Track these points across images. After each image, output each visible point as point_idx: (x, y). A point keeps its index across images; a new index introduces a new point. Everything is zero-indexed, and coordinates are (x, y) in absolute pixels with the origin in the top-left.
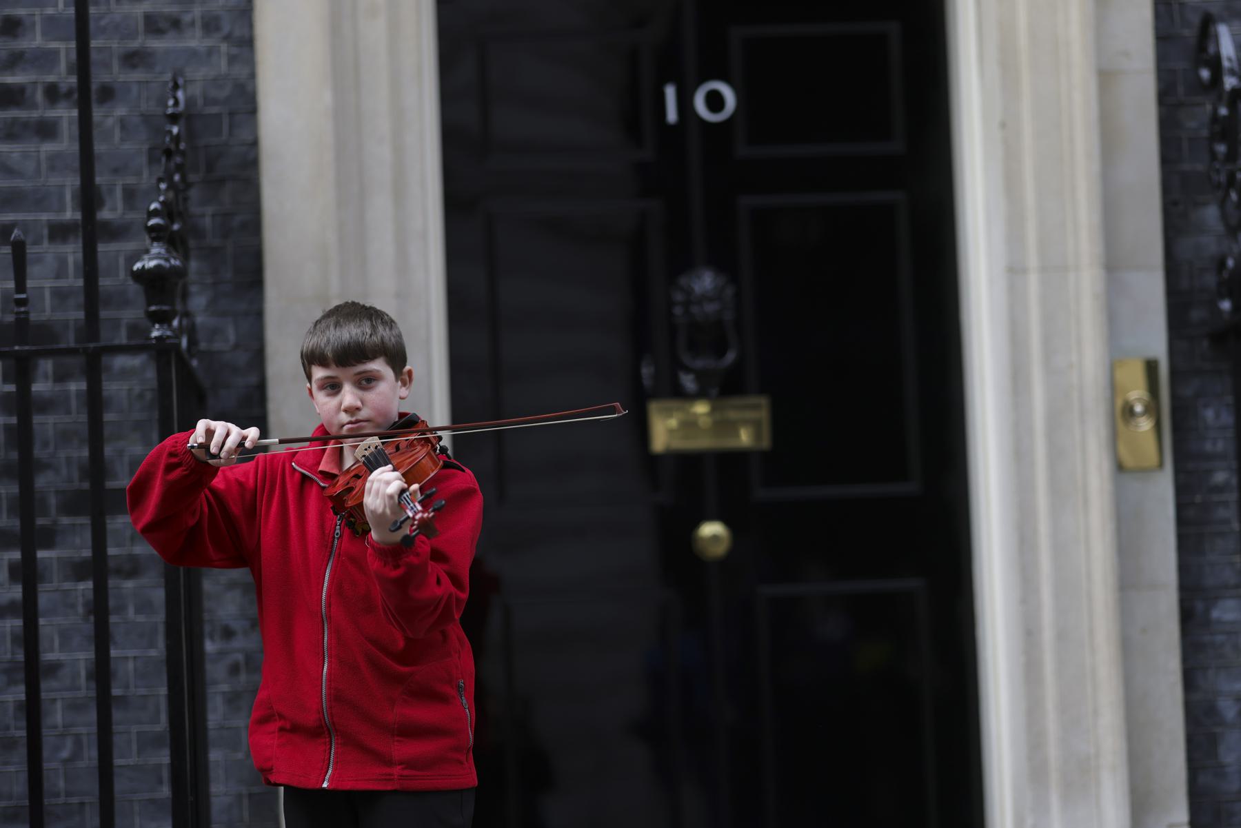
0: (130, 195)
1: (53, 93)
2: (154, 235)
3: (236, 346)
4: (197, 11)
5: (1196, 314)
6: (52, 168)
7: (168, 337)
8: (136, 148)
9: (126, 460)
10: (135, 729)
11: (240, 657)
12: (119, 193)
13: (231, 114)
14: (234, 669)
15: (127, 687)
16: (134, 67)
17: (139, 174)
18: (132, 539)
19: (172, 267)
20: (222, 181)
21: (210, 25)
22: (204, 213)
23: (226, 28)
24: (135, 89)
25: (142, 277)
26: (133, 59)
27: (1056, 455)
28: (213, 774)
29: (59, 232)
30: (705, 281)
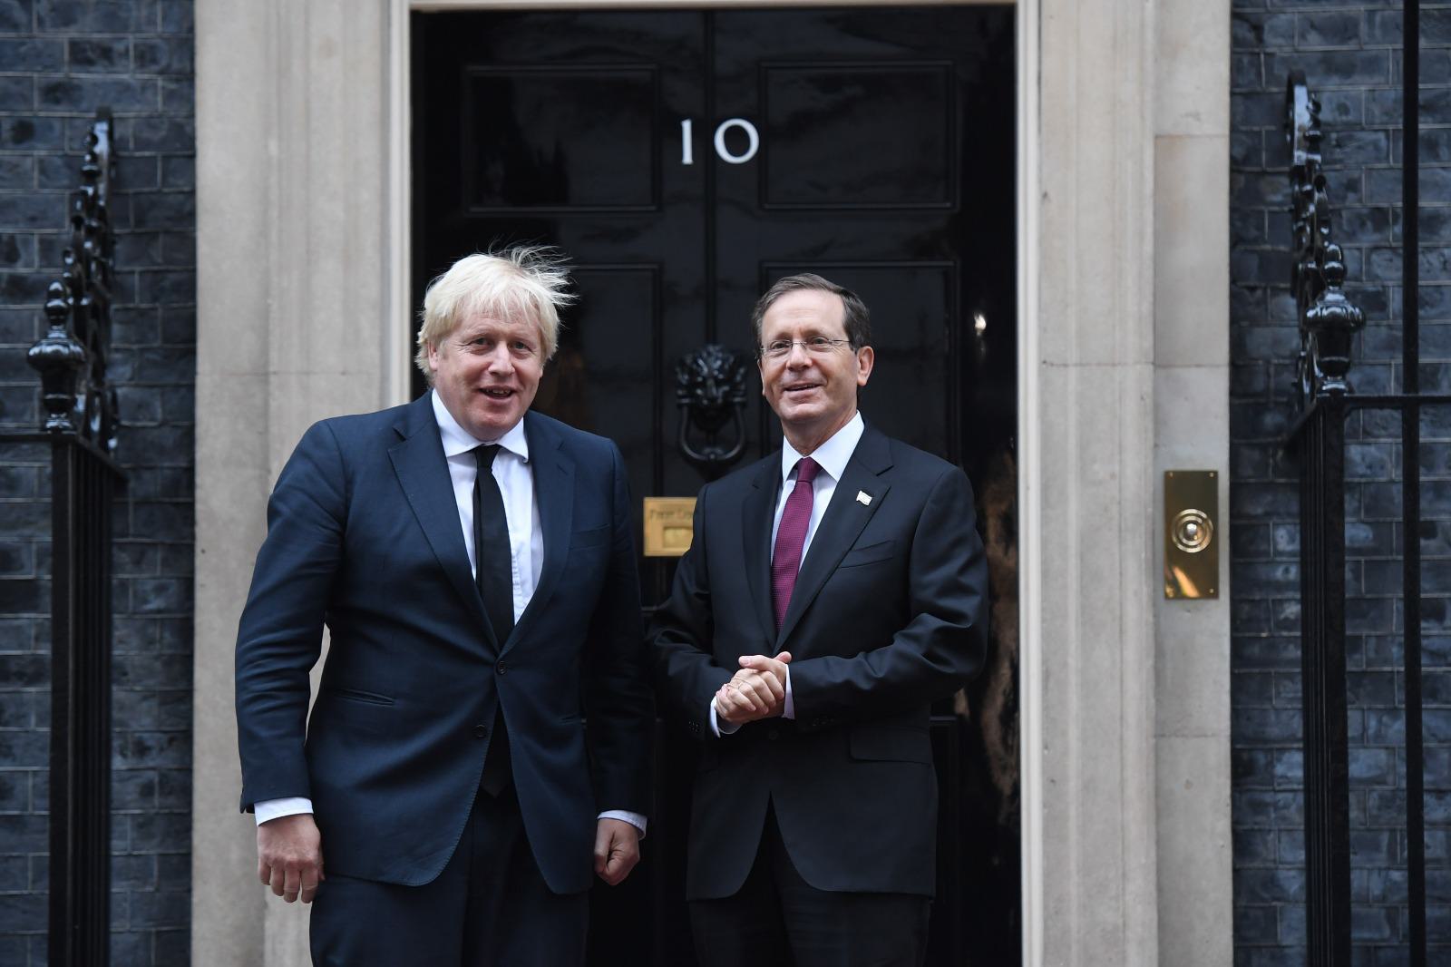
0: (47, 246)
2: (53, 317)
3: (162, 425)
4: (131, 39)
5: (1271, 420)
7: (65, 428)
8: (56, 196)
9: (34, 547)
10: (31, 855)
11: (154, 776)
12: (36, 246)
13: (166, 158)
14: (147, 791)
15: (25, 808)
16: (57, 101)
17: (59, 225)
18: (37, 639)
19: (73, 353)
20: (153, 236)
21: (145, 56)
22: (131, 269)
24: (57, 125)
25: (42, 362)
26: (56, 93)
28: (115, 909)
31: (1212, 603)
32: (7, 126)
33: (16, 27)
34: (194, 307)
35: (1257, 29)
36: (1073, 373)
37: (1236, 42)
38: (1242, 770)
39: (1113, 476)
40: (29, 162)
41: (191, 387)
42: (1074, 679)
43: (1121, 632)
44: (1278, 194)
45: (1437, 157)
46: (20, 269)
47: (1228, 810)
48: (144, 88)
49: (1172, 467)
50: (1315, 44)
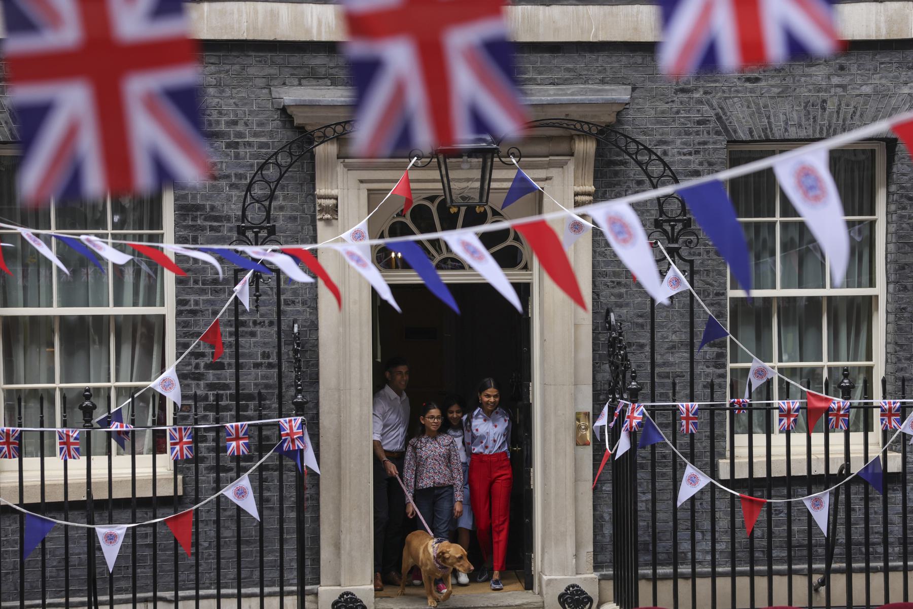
1: (255, 323)
20: (307, 351)
21: (304, 303)
29: (257, 366)
32: (266, 322)
35: (598, 295)
37: (593, 299)
41: (318, 392)
44: (603, 338)
46: (271, 361)
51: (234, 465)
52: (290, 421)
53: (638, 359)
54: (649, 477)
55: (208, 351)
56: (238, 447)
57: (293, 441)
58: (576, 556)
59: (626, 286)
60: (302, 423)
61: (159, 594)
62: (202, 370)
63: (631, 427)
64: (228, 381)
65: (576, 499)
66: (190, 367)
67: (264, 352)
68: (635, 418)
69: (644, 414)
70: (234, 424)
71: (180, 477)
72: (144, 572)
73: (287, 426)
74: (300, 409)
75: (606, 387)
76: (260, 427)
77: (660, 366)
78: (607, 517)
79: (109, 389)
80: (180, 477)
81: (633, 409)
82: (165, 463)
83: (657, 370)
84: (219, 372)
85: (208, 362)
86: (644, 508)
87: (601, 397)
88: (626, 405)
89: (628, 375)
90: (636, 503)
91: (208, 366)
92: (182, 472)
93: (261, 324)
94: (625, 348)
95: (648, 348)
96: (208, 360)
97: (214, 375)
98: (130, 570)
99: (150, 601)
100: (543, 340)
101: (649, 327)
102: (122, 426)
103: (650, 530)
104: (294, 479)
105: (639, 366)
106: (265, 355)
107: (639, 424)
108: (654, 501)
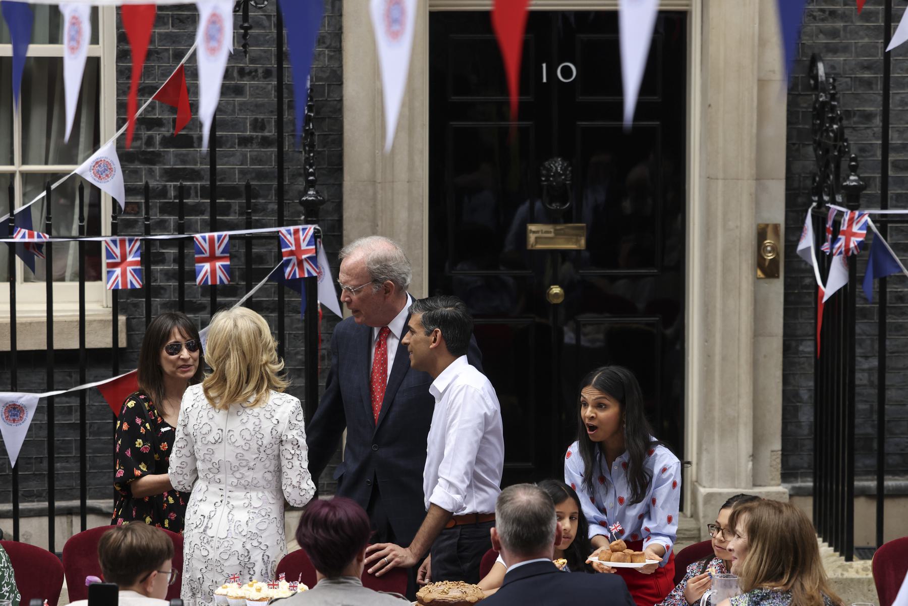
6: (240, 110)
20: (323, 119)
23: (328, 42)
27: (726, 270)
29: (244, 141)
30: (558, 165)
31: (775, 280)
32: (260, 71)
33: (264, 28)
34: (342, 150)
36: (720, 183)
38: (787, 349)
39: (737, 227)
40: (270, 87)
41: (340, 185)
42: (719, 313)
43: (740, 294)
44: (805, 104)
45: (872, 89)
46: (267, 134)
47: (781, 367)
48: (319, 55)
49: (760, 222)
50: (823, 40)
51: (206, 300)
52: (296, 231)
53: (863, 138)
54: (874, 330)
55: (167, 116)
56: (213, 272)
57: (300, 263)
58: (754, 457)
59: (844, 17)
60: (315, 236)
61: (90, 503)
62: (158, 148)
63: (847, 249)
64: (198, 166)
65: (755, 365)
66: (138, 143)
67: (256, 120)
68: (855, 235)
69: (869, 229)
70: (207, 235)
71: (122, 318)
72: (66, 467)
73: (291, 239)
74: (312, 213)
75: (809, 183)
76: (248, 241)
77: (898, 149)
78: (805, 395)
79: (12, 175)
80: (122, 318)
81: (851, 221)
82: (99, 298)
83: (892, 157)
84: (184, 151)
85: (167, 134)
86: (865, 382)
87: (800, 200)
88: (841, 214)
89: (844, 165)
90: (853, 372)
91: (168, 142)
92: (124, 312)
93: (252, 74)
94: (841, 119)
95: (878, 121)
96: (167, 131)
97: (176, 155)
98: (45, 464)
99: (76, 514)
100: (707, 106)
101: (880, 86)
102: (31, 236)
103: (875, 417)
104: (301, 325)
105: (862, 150)
106: (258, 125)
107: (861, 245)
108: (882, 369)
